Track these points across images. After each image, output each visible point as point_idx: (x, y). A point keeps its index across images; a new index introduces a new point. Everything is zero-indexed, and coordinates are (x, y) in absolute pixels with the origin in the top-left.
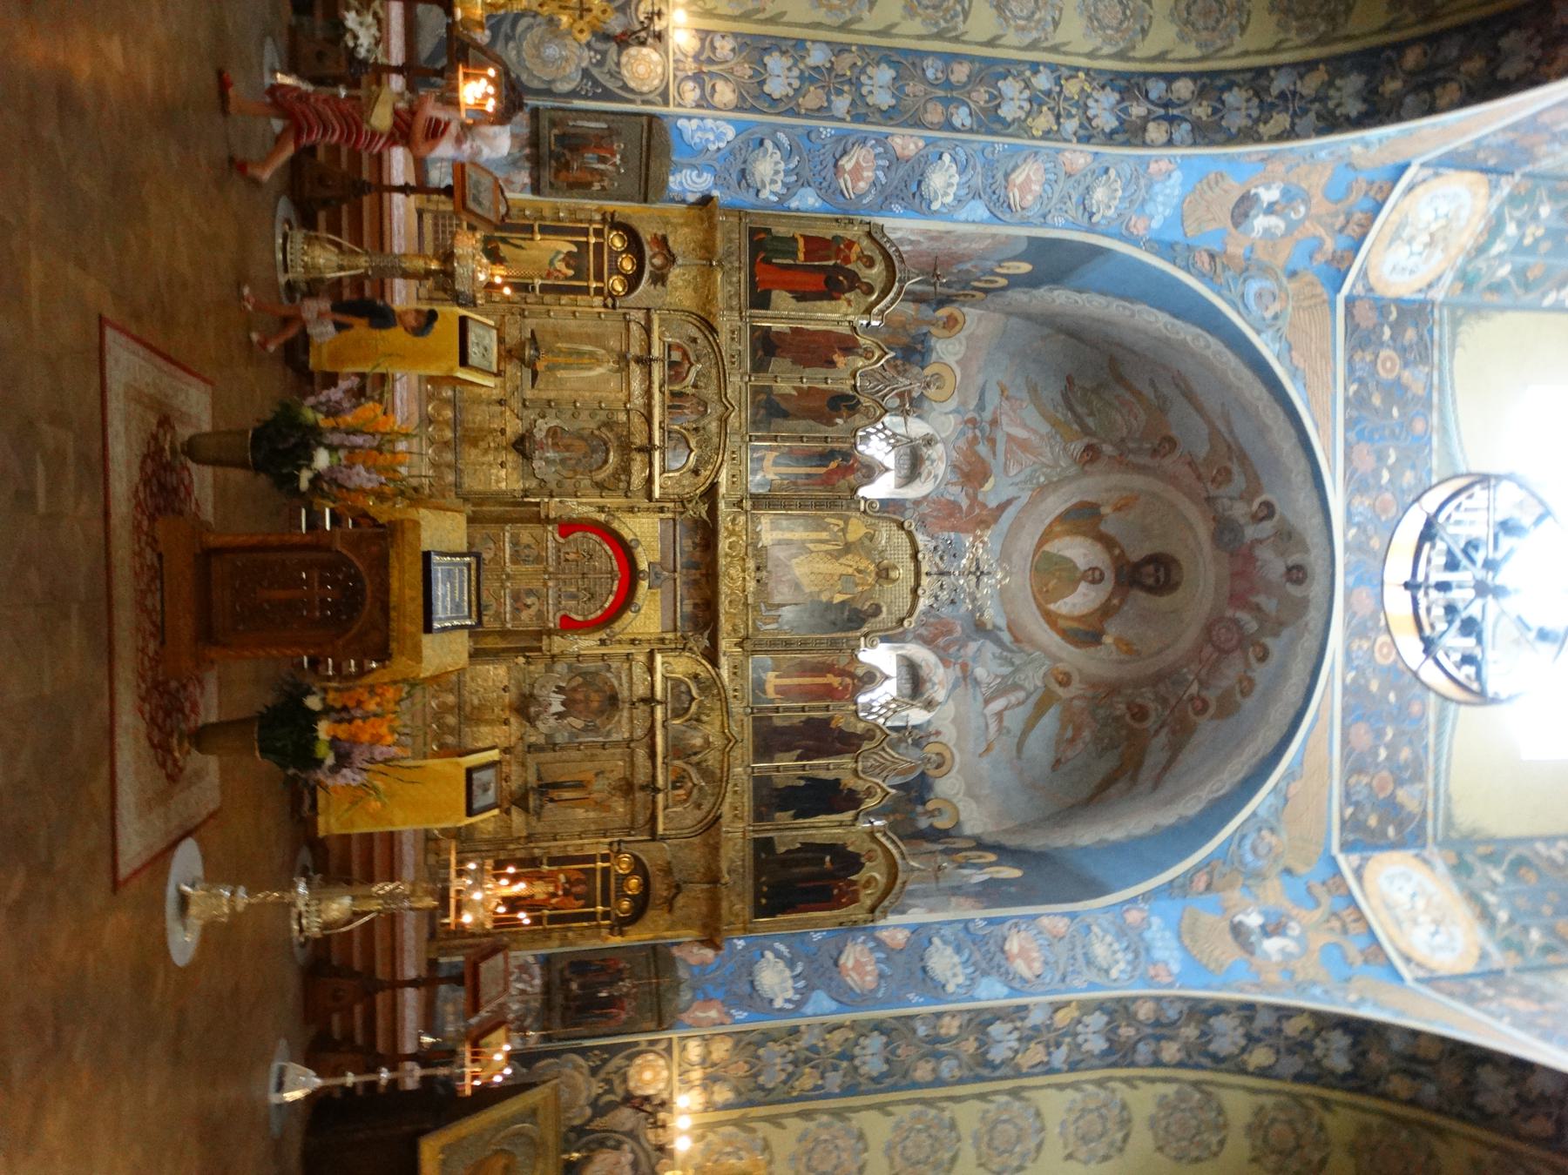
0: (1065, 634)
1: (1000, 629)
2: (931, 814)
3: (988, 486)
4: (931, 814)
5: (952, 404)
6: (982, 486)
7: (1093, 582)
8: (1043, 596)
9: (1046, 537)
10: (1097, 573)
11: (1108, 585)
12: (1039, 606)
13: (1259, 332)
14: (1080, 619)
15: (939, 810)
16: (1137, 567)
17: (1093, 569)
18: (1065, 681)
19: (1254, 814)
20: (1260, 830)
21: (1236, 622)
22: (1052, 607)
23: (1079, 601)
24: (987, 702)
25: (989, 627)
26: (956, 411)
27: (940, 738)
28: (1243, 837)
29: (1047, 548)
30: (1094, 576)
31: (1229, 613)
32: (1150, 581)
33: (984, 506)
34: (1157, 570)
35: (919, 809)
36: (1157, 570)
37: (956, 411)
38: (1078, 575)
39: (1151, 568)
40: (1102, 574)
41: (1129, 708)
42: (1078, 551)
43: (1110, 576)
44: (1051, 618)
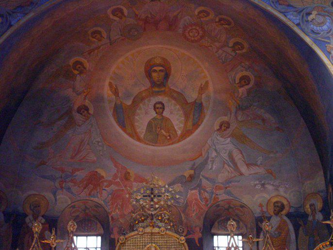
0: (196, 125)
1: (194, 164)
2: (314, 211)
3: (103, 173)
4: (314, 211)
5: (49, 195)
6: (103, 177)
7: (164, 109)
8: (172, 138)
9: (134, 135)
10: (158, 106)
11: (164, 99)
12: (179, 141)
13: (11, 26)
14: (187, 116)
15: (311, 206)
16: (154, 84)
17: (155, 108)
18: (224, 127)
19: (298, 25)
20: (307, 21)
21: (185, 27)
22: (179, 132)
23: (176, 118)
24: (241, 174)
25: (192, 172)
26: (54, 194)
27: (264, 204)
28: (313, 32)
29: (142, 136)
30: (159, 108)
31: (180, 31)
32: (163, 74)
33: (115, 176)
34: (155, 71)
35: (310, 218)
36: (155, 71)
37: (54, 194)
38: (158, 117)
39: (154, 75)
40: (161, 103)
41: (243, 86)
42: (144, 117)
43: (160, 98)
44: (187, 133)
